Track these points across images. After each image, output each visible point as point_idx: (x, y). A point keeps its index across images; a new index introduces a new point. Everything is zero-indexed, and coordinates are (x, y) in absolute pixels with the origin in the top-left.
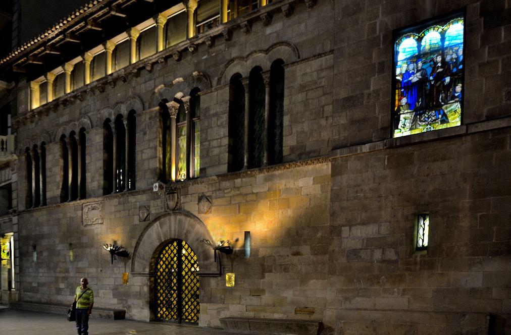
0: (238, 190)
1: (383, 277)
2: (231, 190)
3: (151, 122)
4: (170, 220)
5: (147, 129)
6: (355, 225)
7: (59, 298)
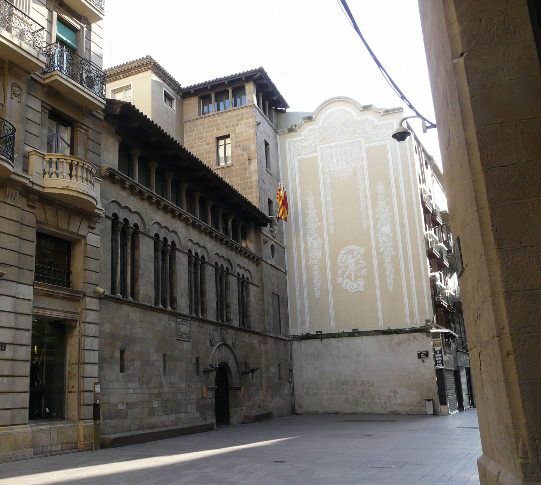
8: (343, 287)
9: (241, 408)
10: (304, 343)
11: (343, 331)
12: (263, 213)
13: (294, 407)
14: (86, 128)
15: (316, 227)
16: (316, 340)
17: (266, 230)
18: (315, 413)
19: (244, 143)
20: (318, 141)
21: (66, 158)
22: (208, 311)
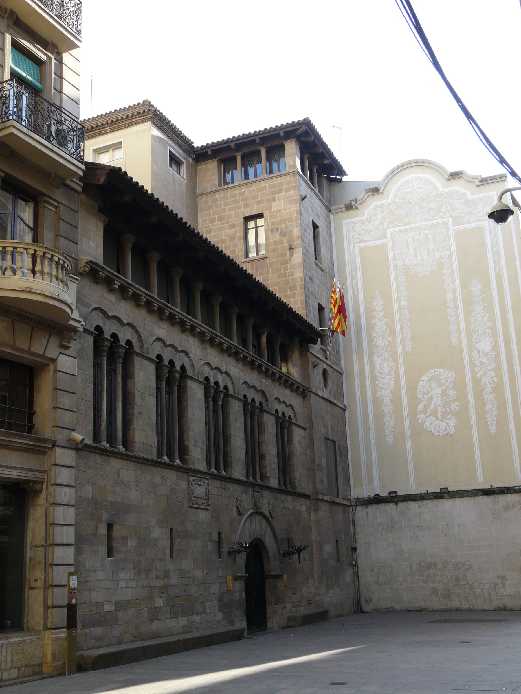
8: (425, 428)
9: (283, 606)
10: (372, 509)
11: (427, 491)
12: (311, 325)
13: (359, 603)
14: (56, 204)
15: (387, 343)
16: (388, 504)
17: (316, 349)
18: (390, 610)
19: (283, 226)
20: (388, 222)
21: (26, 247)
22: (233, 465)
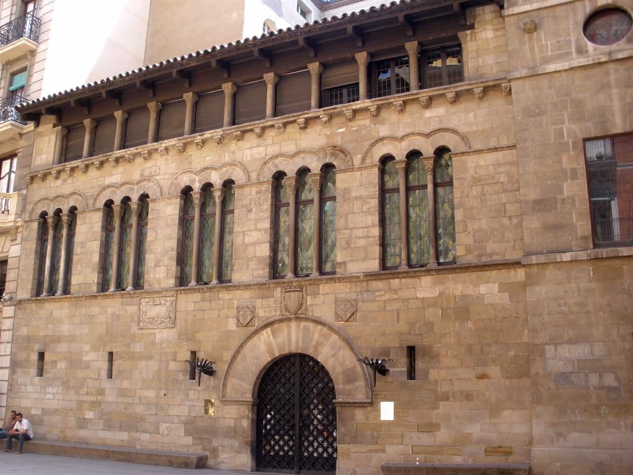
0: (396, 294)
1: (604, 407)
2: (385, 292)
3: (259, 198)
4: (289, 328)
5: (253, 205)
6: (562, 344)
7: (83, 433)
9: (373, 447)
12: (372, 9)
